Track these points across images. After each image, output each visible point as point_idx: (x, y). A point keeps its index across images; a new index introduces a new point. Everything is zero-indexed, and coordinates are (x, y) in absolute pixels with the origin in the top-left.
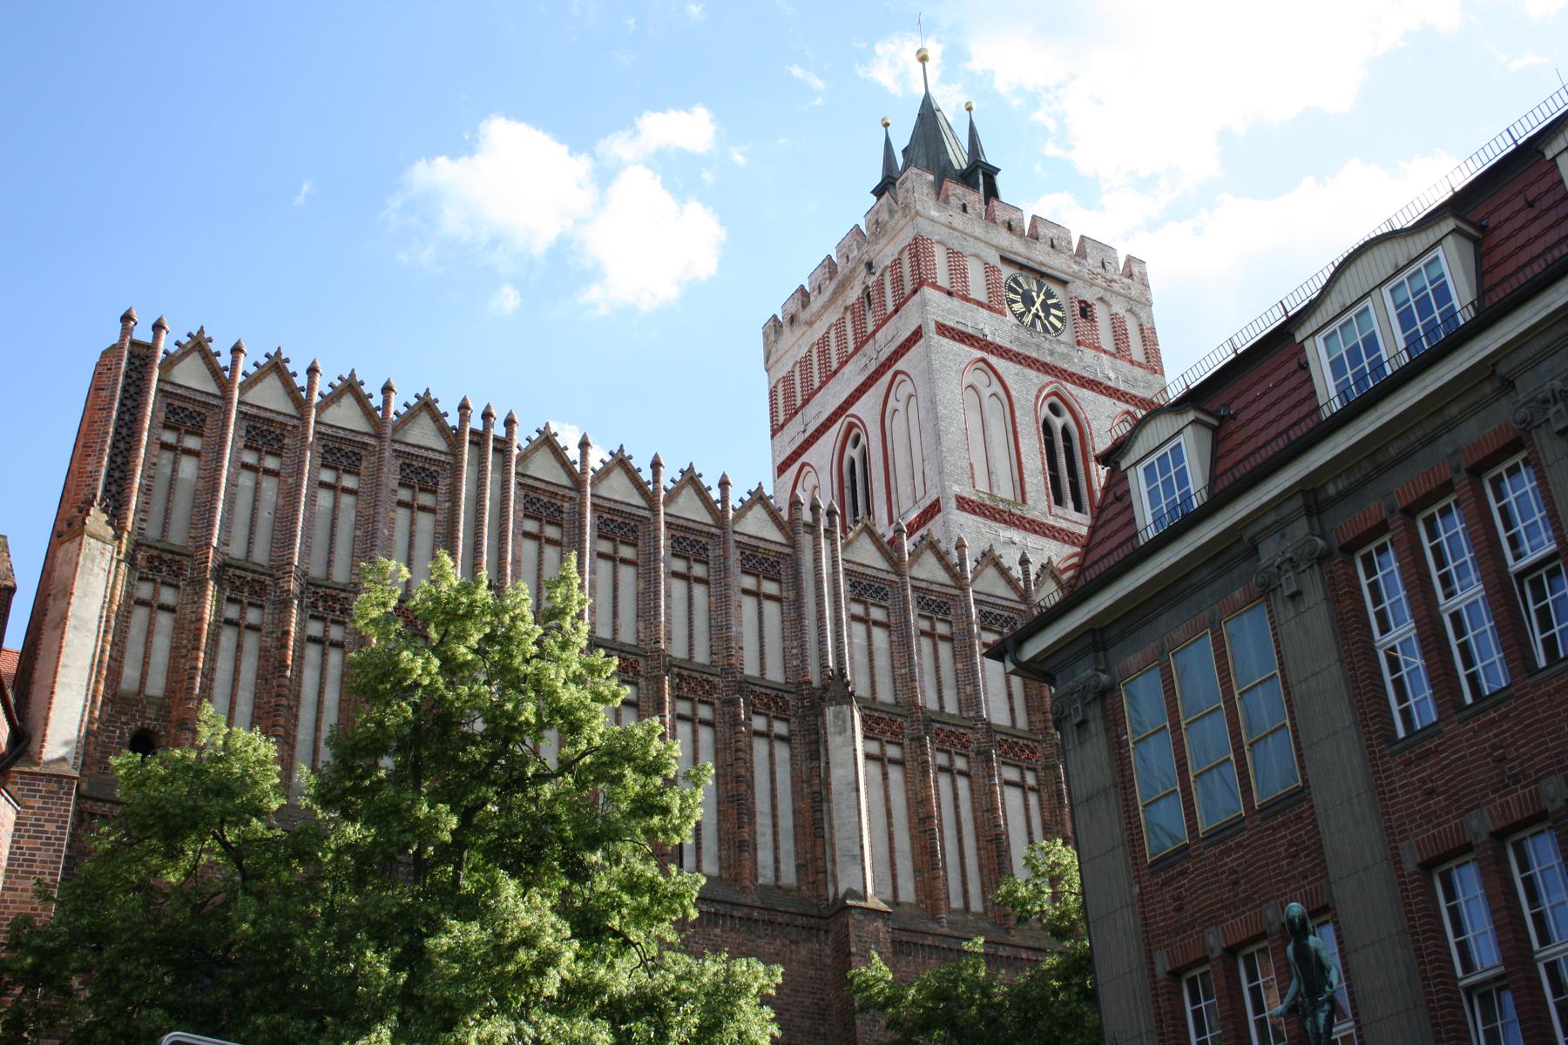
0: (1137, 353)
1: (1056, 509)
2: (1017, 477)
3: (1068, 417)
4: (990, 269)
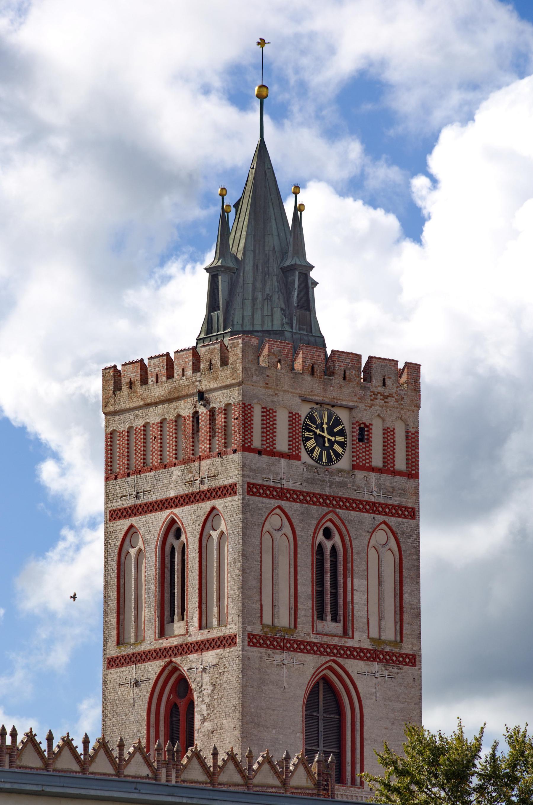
0: (400, 464)
1: (320, 626)
2: (292, 605)
3: (337, 538)
4: (293, 417)
